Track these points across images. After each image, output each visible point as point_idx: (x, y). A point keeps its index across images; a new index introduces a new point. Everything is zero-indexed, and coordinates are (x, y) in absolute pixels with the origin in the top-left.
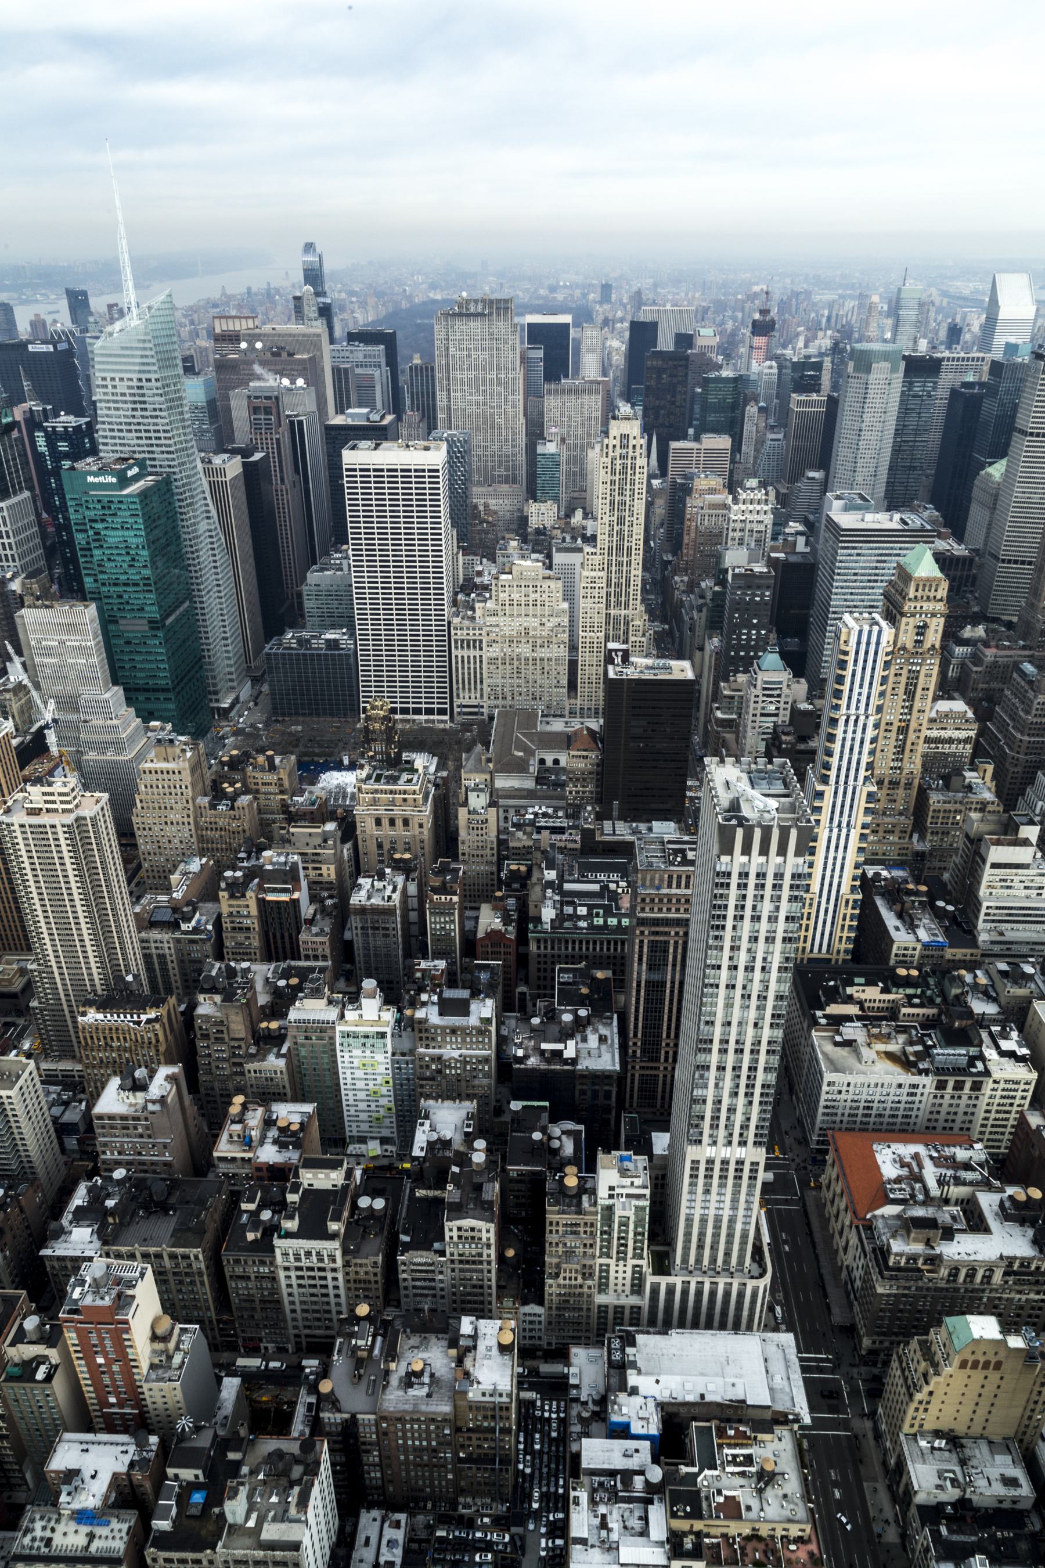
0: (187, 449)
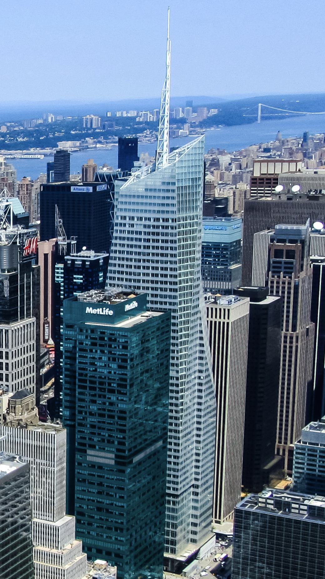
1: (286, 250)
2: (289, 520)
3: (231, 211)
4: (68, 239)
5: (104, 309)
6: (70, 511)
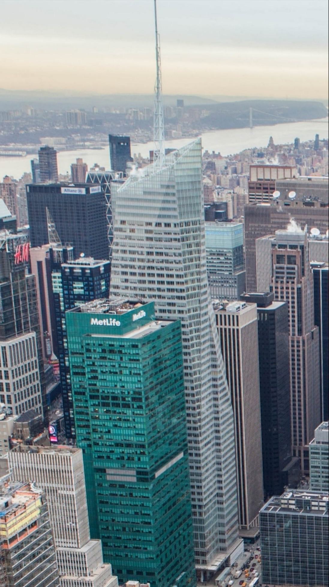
0: (198, 295)
1: (288, 256)
2: (311, 518)
3: (231, 217)
4: (63, 244)
5: (111, 319)
6: (94, 535)
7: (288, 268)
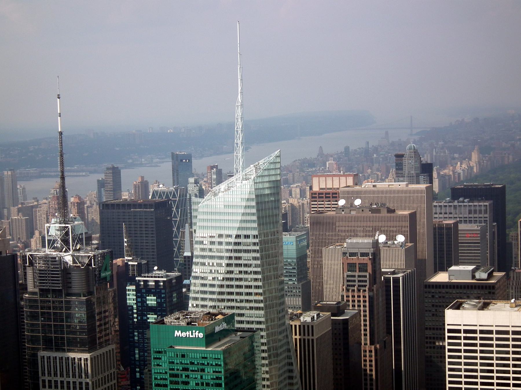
7: (359, 276)
